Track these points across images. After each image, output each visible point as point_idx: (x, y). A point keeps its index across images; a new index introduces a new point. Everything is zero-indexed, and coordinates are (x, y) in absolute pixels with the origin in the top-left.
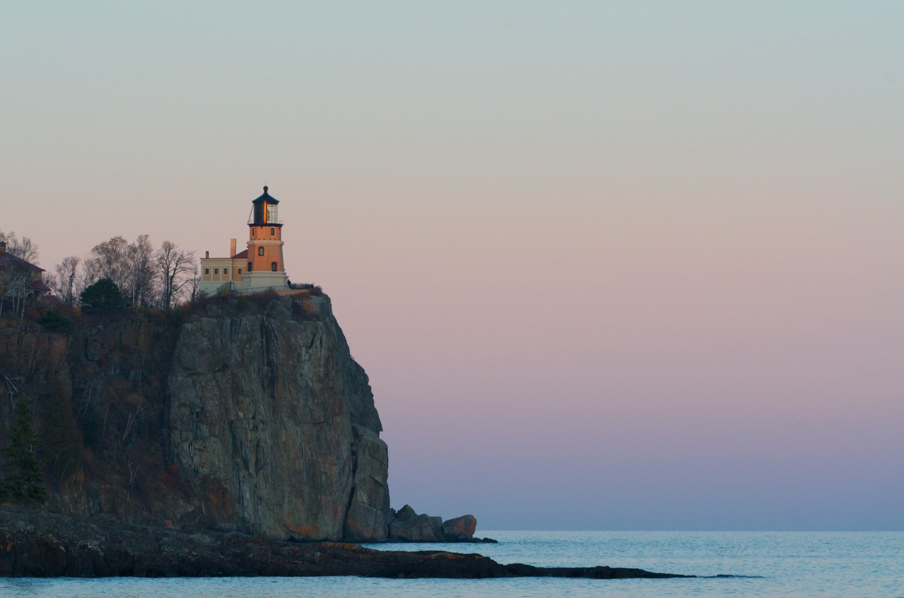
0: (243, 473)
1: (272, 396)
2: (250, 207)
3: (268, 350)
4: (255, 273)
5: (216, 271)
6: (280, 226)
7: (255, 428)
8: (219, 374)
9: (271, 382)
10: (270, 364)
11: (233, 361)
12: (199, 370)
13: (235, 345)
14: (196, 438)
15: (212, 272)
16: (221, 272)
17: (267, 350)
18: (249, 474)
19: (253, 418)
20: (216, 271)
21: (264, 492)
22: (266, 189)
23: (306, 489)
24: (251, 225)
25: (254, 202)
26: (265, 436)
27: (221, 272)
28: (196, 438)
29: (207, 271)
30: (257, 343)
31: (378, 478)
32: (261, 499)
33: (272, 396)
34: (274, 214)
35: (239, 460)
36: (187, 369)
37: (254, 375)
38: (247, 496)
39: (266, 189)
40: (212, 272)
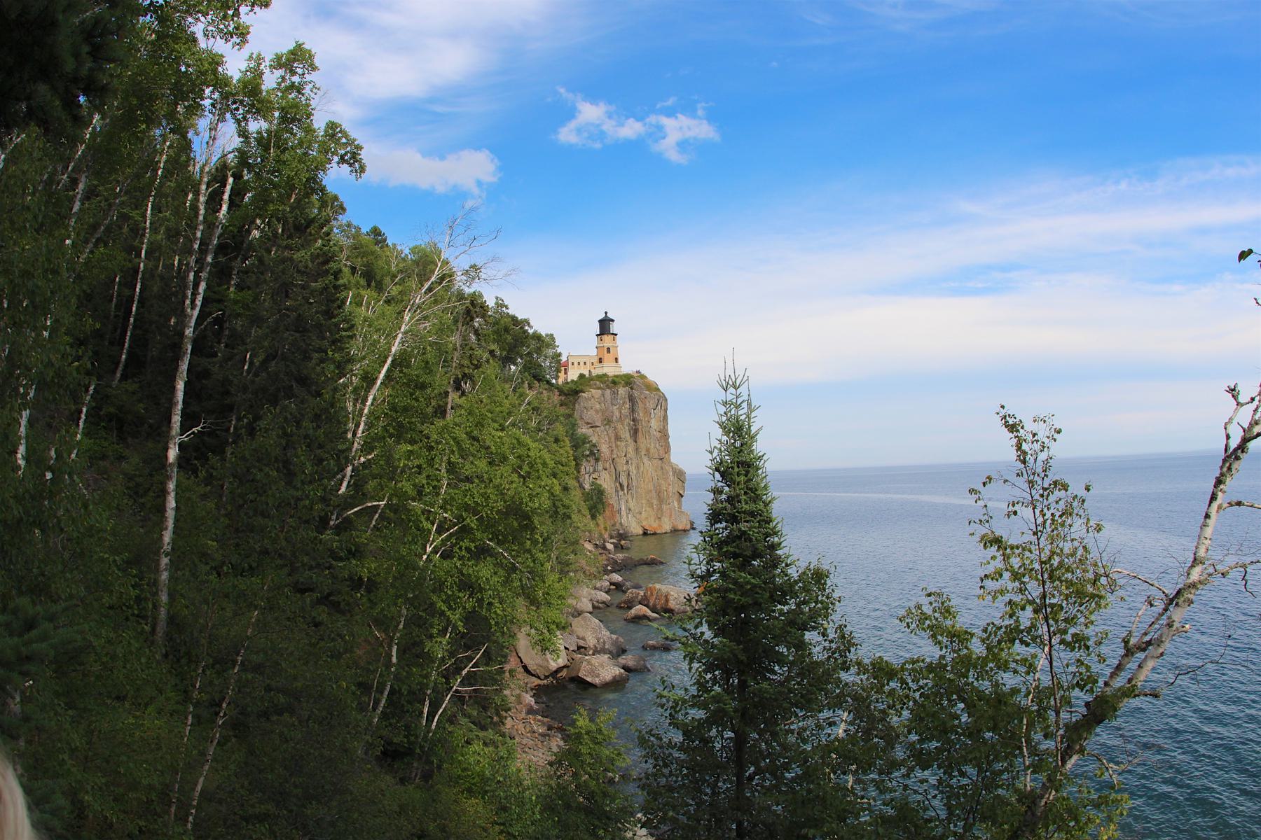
0: (621, 493)
1: (636, 442)
2: (597, 326)
3: (633, 411)
4: (605, 364)
5: (579, 364)
6: (616, 335)
7: (627, 462)
8: (607, 427)
9: (635, 433)
10: (633, 420)
11: (615, 418)
12: (597, 424)
13: (615, 408)
14: (595, 471)
15: (576, 364)
16: (582, 364)
17: (633, 410)
18: (624, 494)
19: (625, 456)
20: (579, 364)
21: (632, 505)
22: (606, 313)
23: (655, 502)
24: (597, 335)
25: (600, 321)
26: (632, 468)
27: (582, 364)
28: (594, 471)
29: (573, 364)
30: (628, 406)
31: (681, 492)
32: (630, 510)
33: (636, 442)
34: (614, 328)
35: (617, 484)
36: (588, 423)
37: (627, 428)
38: (623, 508)
39: (606, 313)
40: (576, 364)
